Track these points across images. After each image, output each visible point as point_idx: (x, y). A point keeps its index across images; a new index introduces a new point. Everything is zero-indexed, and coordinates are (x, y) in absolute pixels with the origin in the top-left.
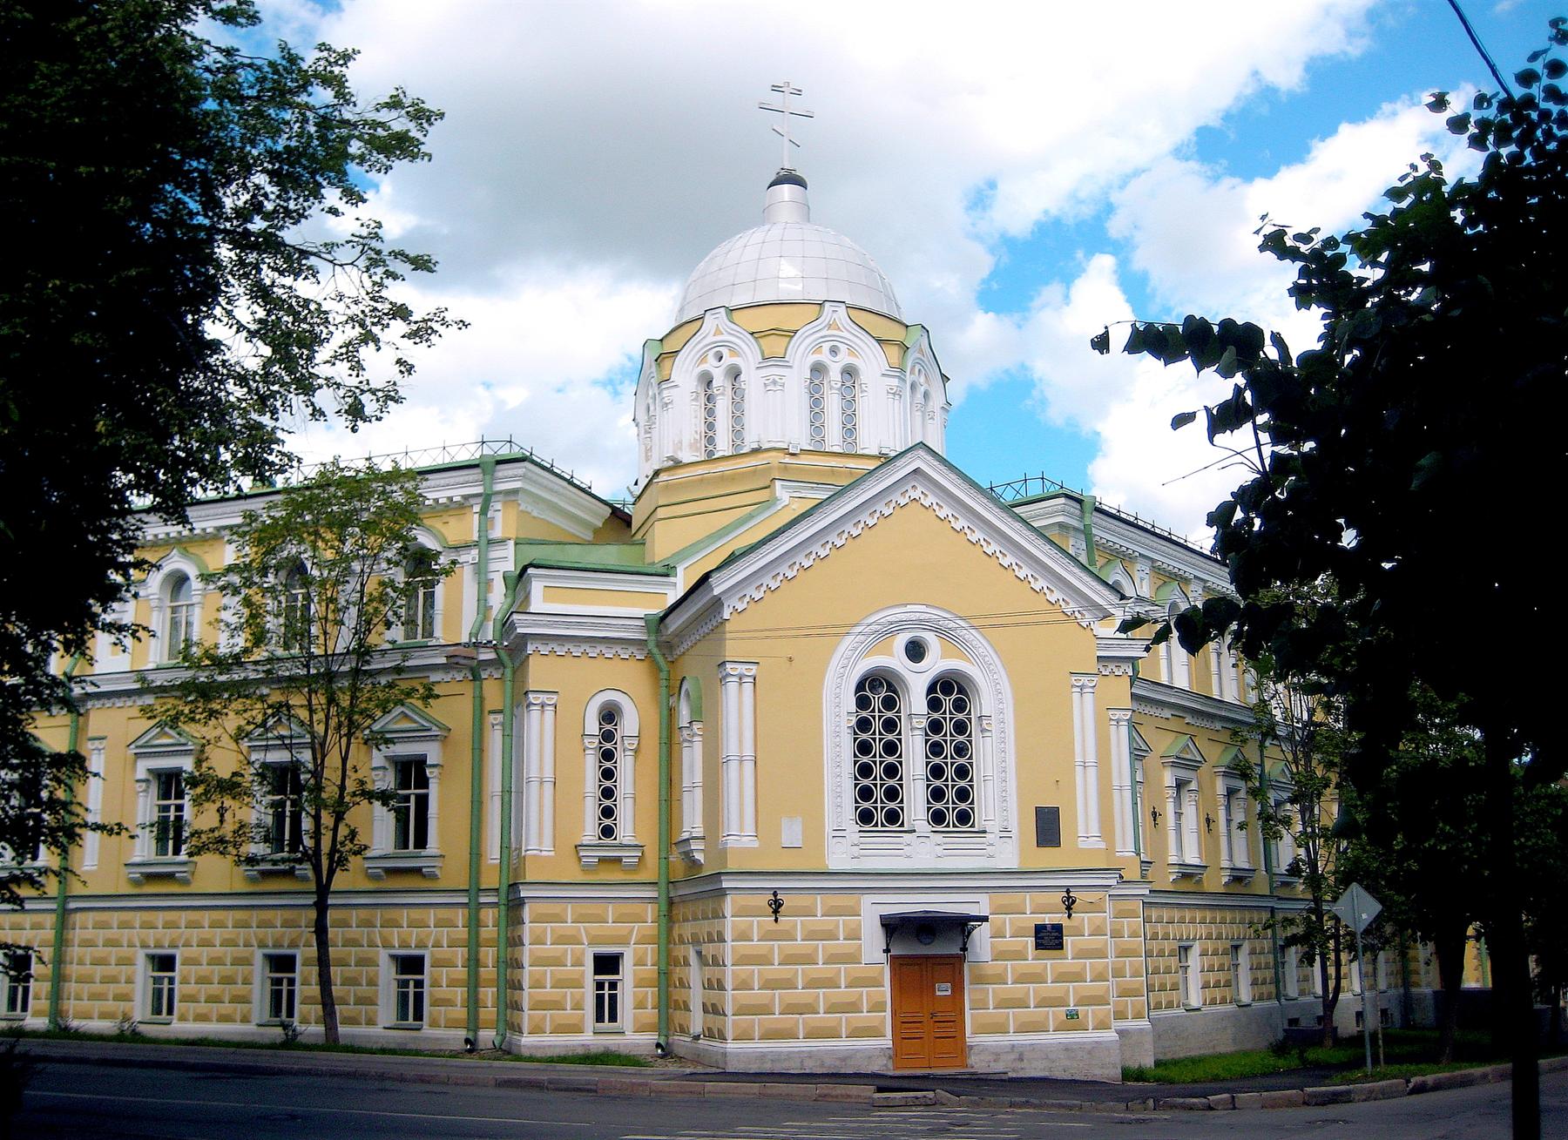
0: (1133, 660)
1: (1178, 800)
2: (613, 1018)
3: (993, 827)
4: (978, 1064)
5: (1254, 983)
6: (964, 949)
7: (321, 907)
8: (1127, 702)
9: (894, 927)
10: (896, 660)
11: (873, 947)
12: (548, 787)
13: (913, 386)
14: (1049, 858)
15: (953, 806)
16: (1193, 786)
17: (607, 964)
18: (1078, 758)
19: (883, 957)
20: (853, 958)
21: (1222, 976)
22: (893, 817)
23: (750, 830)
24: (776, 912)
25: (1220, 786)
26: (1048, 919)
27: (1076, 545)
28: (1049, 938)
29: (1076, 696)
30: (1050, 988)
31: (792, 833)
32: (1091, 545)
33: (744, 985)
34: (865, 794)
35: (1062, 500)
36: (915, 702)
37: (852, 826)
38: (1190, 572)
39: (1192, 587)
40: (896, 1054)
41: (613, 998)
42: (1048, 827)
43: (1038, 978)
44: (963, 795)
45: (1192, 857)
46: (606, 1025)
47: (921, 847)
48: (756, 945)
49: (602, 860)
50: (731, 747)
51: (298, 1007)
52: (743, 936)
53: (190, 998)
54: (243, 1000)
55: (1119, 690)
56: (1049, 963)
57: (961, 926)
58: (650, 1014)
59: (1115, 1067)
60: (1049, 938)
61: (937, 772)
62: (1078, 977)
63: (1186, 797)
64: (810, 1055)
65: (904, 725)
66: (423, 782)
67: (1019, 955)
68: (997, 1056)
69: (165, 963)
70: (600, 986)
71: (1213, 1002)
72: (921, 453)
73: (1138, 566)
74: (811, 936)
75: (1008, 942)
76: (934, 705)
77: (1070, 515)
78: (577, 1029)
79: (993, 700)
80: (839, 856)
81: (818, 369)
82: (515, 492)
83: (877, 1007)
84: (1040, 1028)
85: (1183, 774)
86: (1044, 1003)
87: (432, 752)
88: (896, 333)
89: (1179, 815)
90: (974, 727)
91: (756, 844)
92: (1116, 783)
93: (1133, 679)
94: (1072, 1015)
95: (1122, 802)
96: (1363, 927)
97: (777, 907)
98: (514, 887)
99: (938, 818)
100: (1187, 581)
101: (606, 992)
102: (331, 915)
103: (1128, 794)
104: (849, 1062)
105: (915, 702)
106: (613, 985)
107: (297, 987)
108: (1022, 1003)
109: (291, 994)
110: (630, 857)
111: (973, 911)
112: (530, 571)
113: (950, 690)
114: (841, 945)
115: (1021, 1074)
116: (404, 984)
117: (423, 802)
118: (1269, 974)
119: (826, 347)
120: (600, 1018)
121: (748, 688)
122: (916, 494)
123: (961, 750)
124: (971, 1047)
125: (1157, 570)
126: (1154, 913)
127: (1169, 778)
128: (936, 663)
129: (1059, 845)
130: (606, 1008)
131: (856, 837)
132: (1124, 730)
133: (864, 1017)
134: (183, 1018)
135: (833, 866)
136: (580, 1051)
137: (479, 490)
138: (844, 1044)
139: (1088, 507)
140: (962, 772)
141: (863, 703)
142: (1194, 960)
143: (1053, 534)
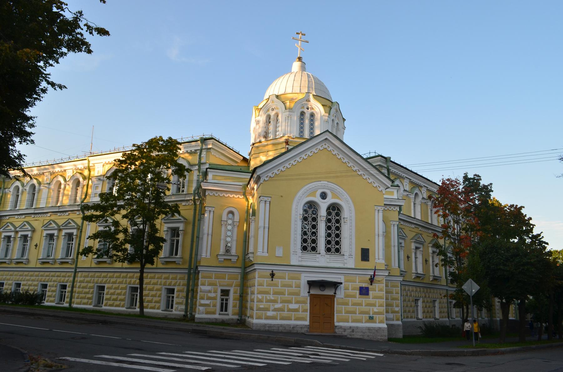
0: (400, 206)
1: (416, 254)
2: (226, 310)
3: (347, 254)
4: (338, 332)
5: (440, 312)
6: (335, 293)
7: (142, 272)
8: (397, 220)
9: (311, 284)
10: (317, 199)
11: (304, 292)
12: (210, 237)
13: (333, 120)
14: (365, 264)
15: (334, 246)
16: (421, 249)
17: (225, 293)
18: (377, 233)
19: (307, 295)
20: (298, 294)
21: (430, 310)
22: (314, 249)
23: (266, 250)
24: (272, 277)
25: (430, 250)
26: (364, 285)
27: (385, 171)
28: (364, 291)
29: (376, 213)
30: (364, 308)
31: (279, 252)
32: (388, 170)
33: (260, 301)
34: (305, 241)
35: (380, 157)
36: (323, 212)
37: (299, 251)
38: (422, 184)
39: (423, 189)
40: (310, 326)
41: (226, 304)
42: (365, 255)
43: (360, 304)
44: (337, 243)
45: (420, 271)
46: (224, 312)
47: (322, 259)
48: (265, 288)
49: (224, 259)
50: (261, 224)
51: (175, 306)
52: (261, 285)
53: (150, 302)
54: (158, 302)
55: (394, 216)
56: (364, 300)
57: (335, 285)
58: (237, 310)
59: (385, 336)
60: (364, 291)
61: (329, 235)
62: (374, 305)
63: (418, 252)
64: (281, 325)
65: (319, 219)
66: (178, 236)
67: (354, 296)
68: (345, 330)
69: (102, 288)
70: (222, 300)
71: (426, 317)
72: (327, 133)
73: (405, 181)
74: (284, 286)
75: (350, 292)
76: (329, 214)
77: (383, 163)
78: (214, 313)
79: (348, 213)
80: (294, 261)
81: (302, 114)
82: (210, 149)
83: (305, 311)
84: (360, 321)
85: (418, 245)
86: (361, 313)
87: (181, 226)
88: (329, 104)
89: (416, 258)
90: (342, 221)
91: (267, 255)
92: (393, 244)
93: (399, 212)
94: (371, 318)
95: (394, 250)
96: (473, 294)
97: (272, 275)
98: (197, 267)
99: (328, 250)
100: (421, 187)
101: (224, 302)
102: (145, 275)
103: (396, 248)
104: (295, 329)
105: (323, 212)
106: (227, 300)
107: (175, 299)
108: (354, 313)
109: (173, 301)
110: (234, 259)
111: (339, 281)
112: (208, 170)
113: (335, 210)
114: (294, 289)
115: (353, 337)
116: (169, 297)
117: (178, 241)
118: (446, 310)
119: (305, 107)
120: (222, 310)
121: (268, 205)
122: (326, 147)
123: (338, 228)
124: (336, 326)
125: (411, 182)
126: (403, 287)
127: (413, 246)
128: (330, 200)
129: (368, 261)
130: (224, 307)
131: (300, 254)
132: (396, 228)
133: (300, 314)
134: (106, 305)
135: (292, 263)
136: (214, 321)
137: (199, 148)
138: (293, 322)
139: (388, 160)
140: (338, 236)
141: (305, 211)
142: (420, 303)
143: (377, 167)
